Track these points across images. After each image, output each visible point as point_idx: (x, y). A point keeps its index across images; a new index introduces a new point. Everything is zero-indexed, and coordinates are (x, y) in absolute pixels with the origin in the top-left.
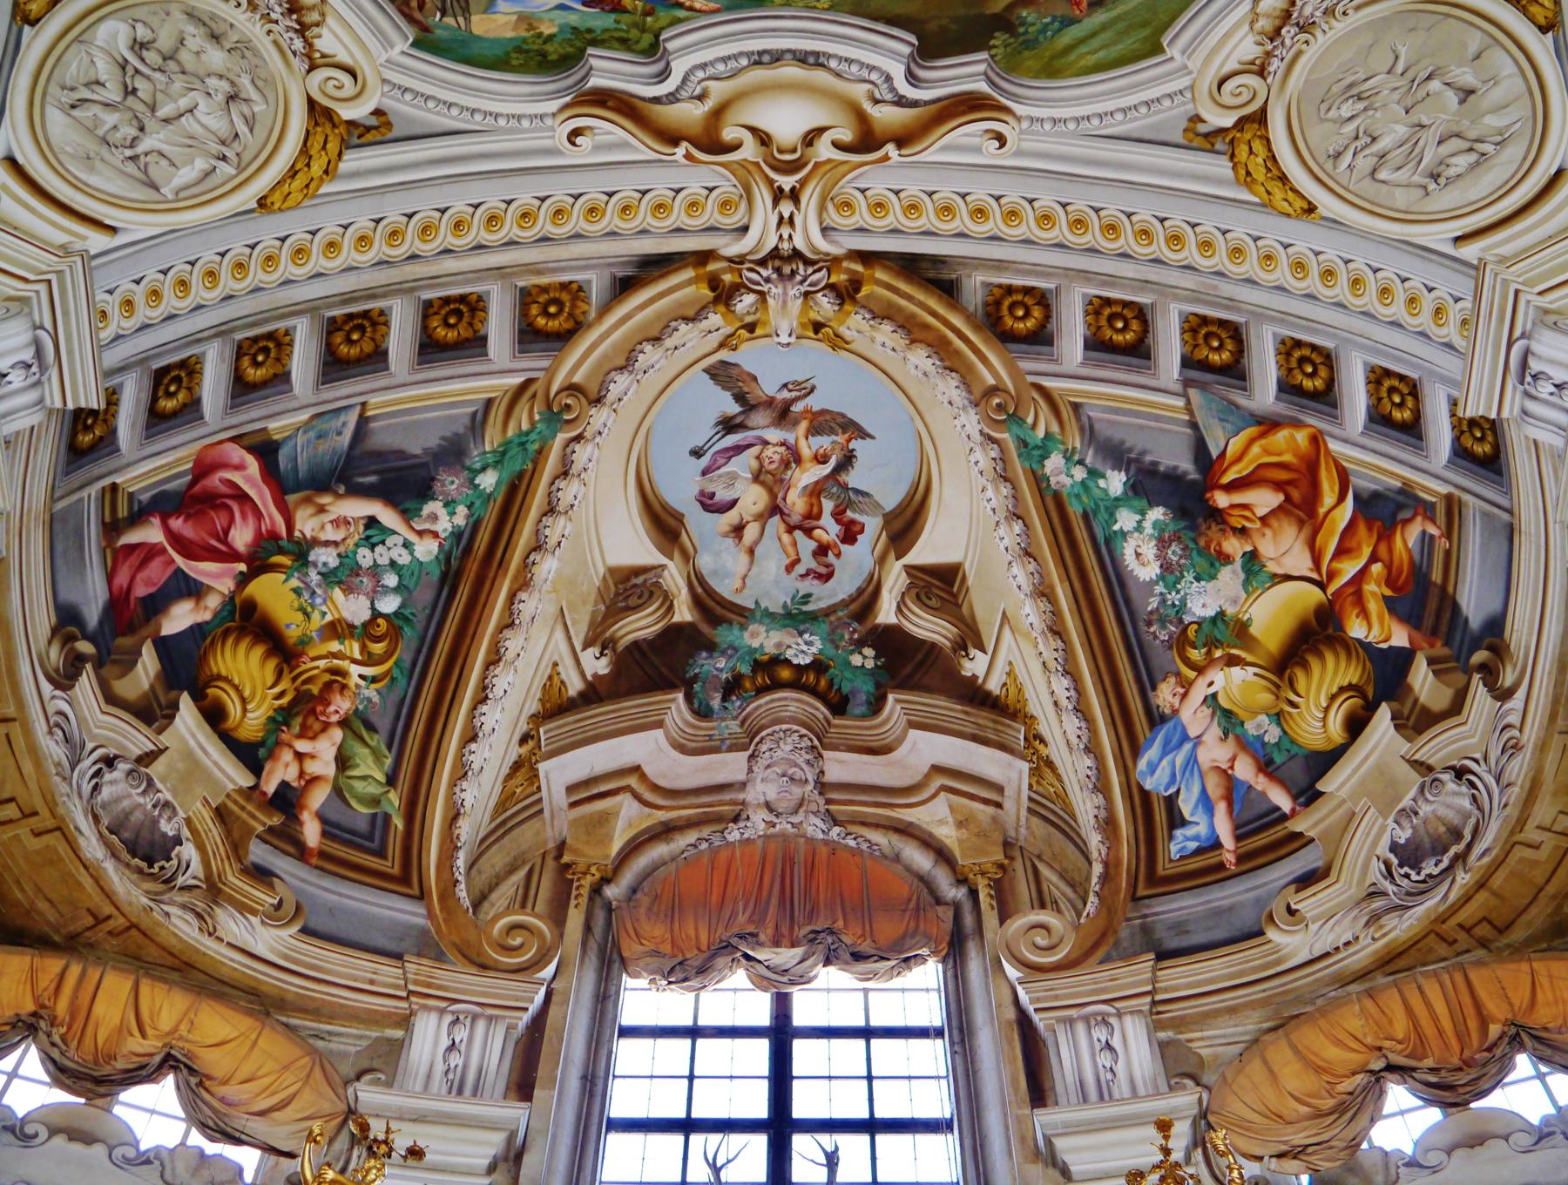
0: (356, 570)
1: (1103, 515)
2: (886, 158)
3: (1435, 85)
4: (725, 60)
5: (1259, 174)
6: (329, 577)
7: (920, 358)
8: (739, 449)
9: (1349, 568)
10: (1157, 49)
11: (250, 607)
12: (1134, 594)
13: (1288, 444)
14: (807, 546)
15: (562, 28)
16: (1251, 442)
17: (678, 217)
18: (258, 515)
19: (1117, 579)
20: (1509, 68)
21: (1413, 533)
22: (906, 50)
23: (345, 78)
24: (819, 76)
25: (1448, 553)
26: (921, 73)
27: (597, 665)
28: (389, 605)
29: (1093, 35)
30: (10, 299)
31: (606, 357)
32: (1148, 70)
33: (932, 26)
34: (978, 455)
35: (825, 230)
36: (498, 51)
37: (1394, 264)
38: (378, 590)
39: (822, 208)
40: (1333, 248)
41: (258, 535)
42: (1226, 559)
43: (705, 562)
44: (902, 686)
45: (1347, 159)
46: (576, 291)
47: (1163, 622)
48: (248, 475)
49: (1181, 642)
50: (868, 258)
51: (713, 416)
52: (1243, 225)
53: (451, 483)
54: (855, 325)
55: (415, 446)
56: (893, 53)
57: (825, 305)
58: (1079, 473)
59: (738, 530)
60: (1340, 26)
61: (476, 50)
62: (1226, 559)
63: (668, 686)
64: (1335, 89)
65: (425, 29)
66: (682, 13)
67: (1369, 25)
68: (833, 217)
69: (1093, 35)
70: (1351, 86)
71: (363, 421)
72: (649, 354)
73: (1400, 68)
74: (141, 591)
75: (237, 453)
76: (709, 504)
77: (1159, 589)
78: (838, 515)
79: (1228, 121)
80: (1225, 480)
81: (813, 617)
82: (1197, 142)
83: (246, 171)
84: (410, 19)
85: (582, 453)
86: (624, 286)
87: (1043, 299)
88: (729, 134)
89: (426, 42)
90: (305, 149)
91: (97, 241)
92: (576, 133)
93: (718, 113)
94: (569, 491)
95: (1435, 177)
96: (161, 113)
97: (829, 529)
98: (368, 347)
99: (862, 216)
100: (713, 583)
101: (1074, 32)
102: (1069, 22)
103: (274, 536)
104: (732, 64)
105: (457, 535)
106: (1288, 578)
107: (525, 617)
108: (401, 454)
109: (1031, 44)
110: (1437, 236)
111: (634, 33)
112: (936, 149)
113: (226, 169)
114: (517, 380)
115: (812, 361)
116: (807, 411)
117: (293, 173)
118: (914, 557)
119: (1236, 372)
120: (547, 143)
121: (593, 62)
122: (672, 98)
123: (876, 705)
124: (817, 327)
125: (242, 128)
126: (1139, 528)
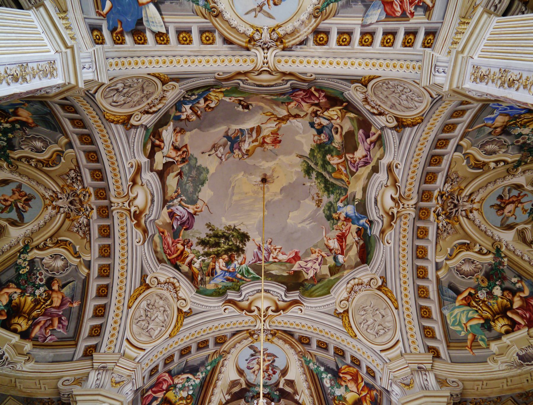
0: (185, 387)
1: (320, 374)
2: (281, 314)
3: (378, 312)
4: (252, 292)
5: (347, 325)
6: (180, 389)
7: (287, 346)
8: (254, 359)
9: (364, 394)
10: (329, 293)
11: (166, 398)
12: (326, 389)
13: (353, 370)
14: (266, 374)
15: (223, 286)
16: (346, 367)
17: (243, 324)
18: (168, 382)
19: (323, 386)
20: (390, 314)
21: (374, 393)
22: (284, 289)
23: (184, 301)
24: (269, 295)
25: (380, 399)
26: (287, 295)
27: (228, 397)
28: (191, 392)
29: (318, 288)
30: (128, 376)
31: (230, 346)
32: (327, 297)
33: (289, 284)
34: (297, 362)
35: (270, 326)
36: (211, 292)
37: (370, 353)
38: (189, 390)
39: (269, 322)
40: (360, 346)
41: (168, 386)
42: (342, 386)
43: (248, 378)
44: (284, 398)
45: (362, 325)
46: (225, 336)
47: (331, 395)
48: (167, 377)
49: (334, 399)
50: (277, 330)
51: (250, 354)
52: (344, 337)
53: (202, 369)
54: (275, 340)
55: (196, 364)
56: (282, 290)
57: (270, 337)
58: (316, 367)
59: (254, 372)
60: (362, 293)
61: (207, 292)
62: (342, 386)
63: (241, 398)
64: (361, 307)
65: (198, 289)
66: (244, 282)
67: (366, 295)
68: (271, 324)
69: (318, 288)
70: (363, 307)
71: (187, 362)
72: (238, 345)
73: (372, 306)
74: (147, 403)
75: (164, 374)
76: (249, 368)
77: (330, 389)
78: (272, 370)
79: (342, 311)
80: (342, 372)
81: (268, 386)
82: (336, 315)
83: (167, 328)
84: (195, 287)
85: (226, 362)
86: (234, 334)
87: (309, 338)
88: (253, 308)
89: (199, 292)
90: (177, 321)
91: (142, 353)
92: (225, 309)
93: (251, 304)
94: (223, 369)
95: (377, 334)
96: (152, 319)
97: (270, 372)
98: (188, 351)
99: (277, 324)
100: (250, 381)
101: (315, 288)
102: (314, 285)
103: (170, 385)
104: (253, 293)
105: (203, 378)
106: (353, 391)
107: (215, 393)
108: (193, 365)
109: (307, 290)
110: (377, 348)
111: (236, 287)
112: (289, 313)
113: (164, 329)
114: (214, 351)
115: (268, 345)
116: (266, 353)
117: (175, 326)
118: (286, 377)
119: (343, 356)
120: (220, 312)
121: (228, 293)
122: (242, 300)
123: (279, 401)
124: (268, 340)
125: (166, 318)
126: (326, 377)
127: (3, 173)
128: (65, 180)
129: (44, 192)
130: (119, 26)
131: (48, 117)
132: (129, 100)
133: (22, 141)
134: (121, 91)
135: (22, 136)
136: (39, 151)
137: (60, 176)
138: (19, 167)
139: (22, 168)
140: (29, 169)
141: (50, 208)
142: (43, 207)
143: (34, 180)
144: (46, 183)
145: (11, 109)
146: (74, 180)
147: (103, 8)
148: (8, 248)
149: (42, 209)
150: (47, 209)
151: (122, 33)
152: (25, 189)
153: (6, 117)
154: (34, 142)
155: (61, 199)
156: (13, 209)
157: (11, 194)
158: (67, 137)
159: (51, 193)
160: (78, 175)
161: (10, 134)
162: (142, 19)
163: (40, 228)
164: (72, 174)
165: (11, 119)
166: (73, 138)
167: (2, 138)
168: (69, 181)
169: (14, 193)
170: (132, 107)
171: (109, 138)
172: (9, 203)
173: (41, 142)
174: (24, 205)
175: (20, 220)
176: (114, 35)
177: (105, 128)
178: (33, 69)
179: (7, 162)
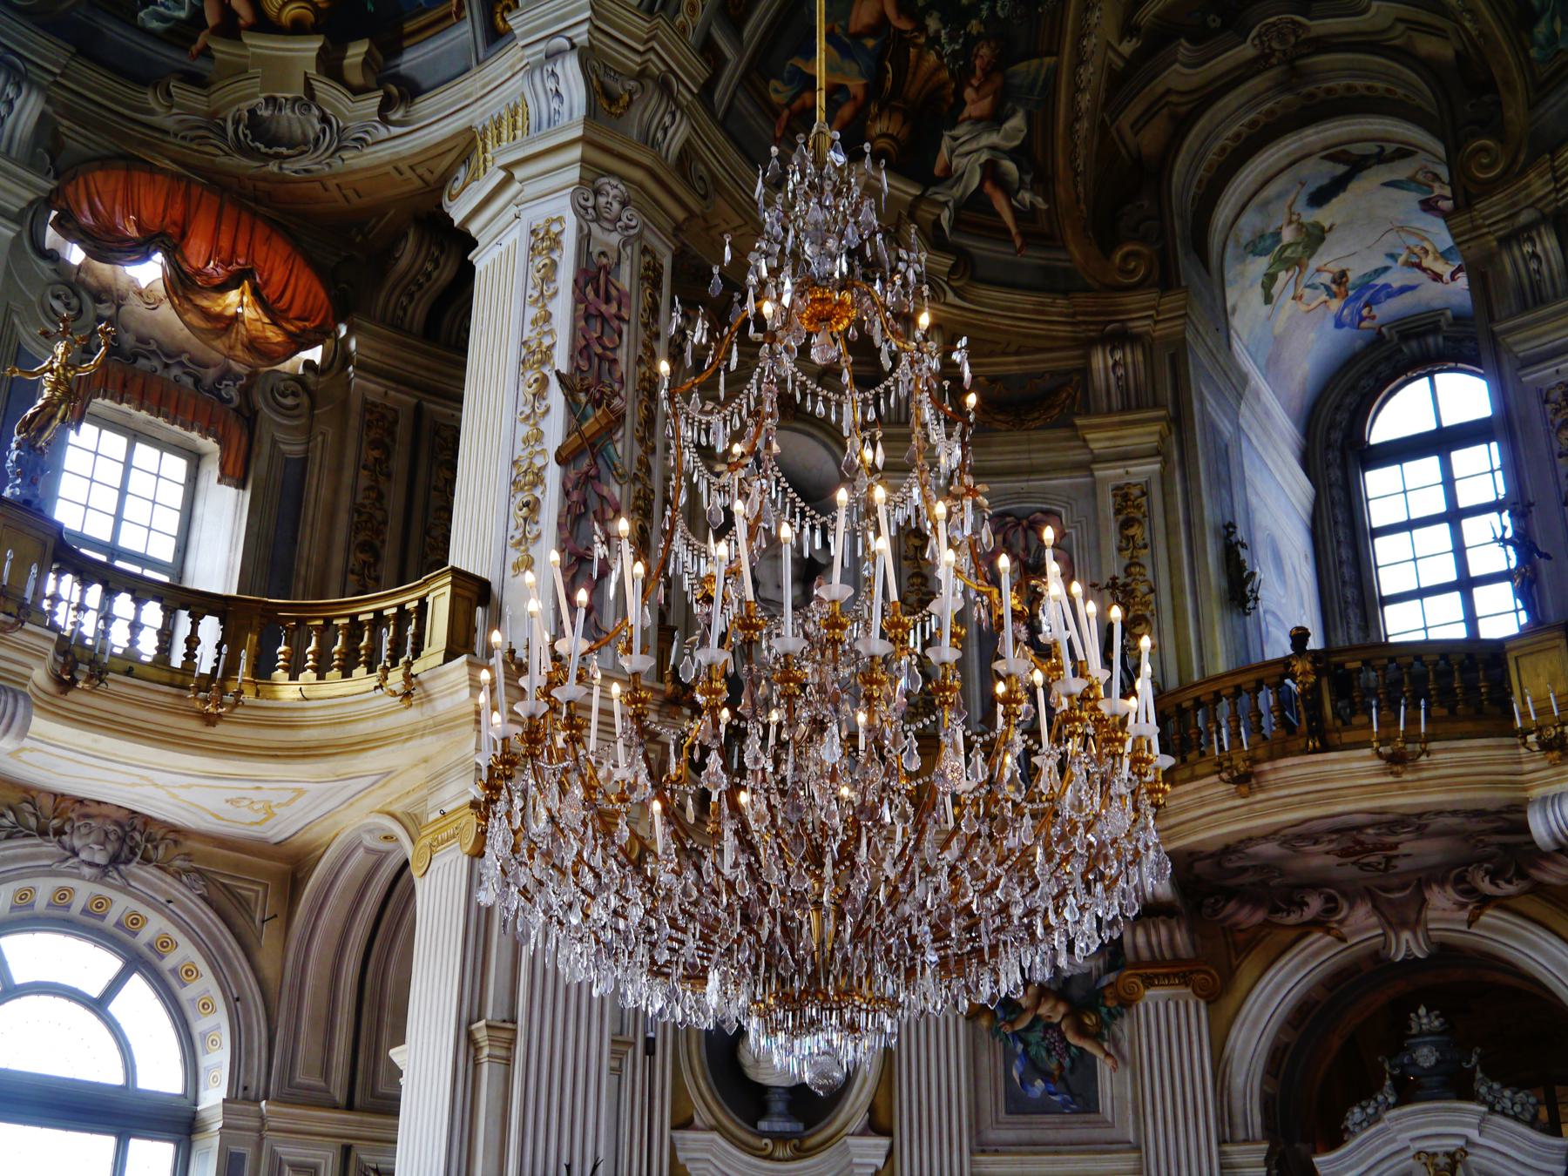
145: (864, 47)
165: (904, 25)
167: (984, 13)
178: (535, 322)
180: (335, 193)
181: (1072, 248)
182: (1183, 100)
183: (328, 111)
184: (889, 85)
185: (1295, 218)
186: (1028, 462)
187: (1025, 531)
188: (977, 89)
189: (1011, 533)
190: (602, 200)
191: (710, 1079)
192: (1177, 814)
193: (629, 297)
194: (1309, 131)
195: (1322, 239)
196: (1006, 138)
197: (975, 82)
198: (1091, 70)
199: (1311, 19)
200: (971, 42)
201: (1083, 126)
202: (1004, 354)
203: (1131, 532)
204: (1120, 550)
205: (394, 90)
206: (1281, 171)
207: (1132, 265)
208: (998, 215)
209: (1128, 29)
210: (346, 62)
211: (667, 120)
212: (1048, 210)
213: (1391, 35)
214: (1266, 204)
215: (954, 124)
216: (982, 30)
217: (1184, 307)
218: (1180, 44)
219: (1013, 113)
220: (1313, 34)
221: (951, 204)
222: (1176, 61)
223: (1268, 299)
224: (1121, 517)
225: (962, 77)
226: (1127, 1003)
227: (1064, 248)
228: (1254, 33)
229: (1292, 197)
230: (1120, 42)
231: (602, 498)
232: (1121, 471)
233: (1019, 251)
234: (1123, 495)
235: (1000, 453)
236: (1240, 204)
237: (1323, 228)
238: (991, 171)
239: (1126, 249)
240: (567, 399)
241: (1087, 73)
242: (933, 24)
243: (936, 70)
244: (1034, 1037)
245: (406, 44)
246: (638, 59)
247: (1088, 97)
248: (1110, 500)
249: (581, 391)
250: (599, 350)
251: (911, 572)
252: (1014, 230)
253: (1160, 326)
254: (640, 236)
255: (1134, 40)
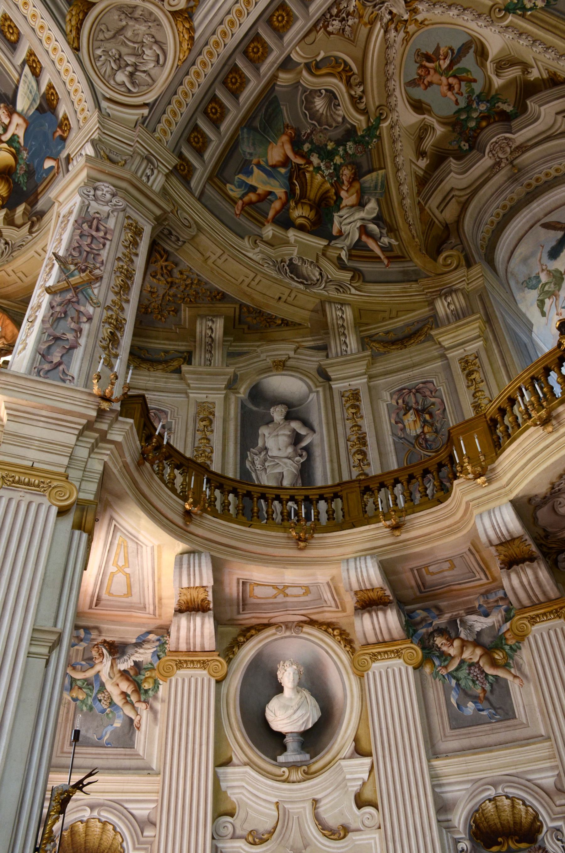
127: (400, 118)
128: (354, 29)
129: (397, 45)
130: (57, 134)
131: (257, 123)
132: (147, 40)
133: (331, 126)
134: (135, 66)
135: (321, 131)
136: (331, 96)
137: (353, 41)
138: (377, 104)
139: (376, 99)
140: (372, 90)
141: (420, 18)
142: (426, 28)
143: (386, 73)
144: (379, 52)
145: (279, 172)
146: (344, 15)
147: (52, 168)
148: (524, 37)
149: (430, 27)
150: (425, 20)
151: (60, 126)
152: (413, 72)
153: (300, 169)
154: (321, 111)
155: (391, 13)
156: (458, 69)
157: (435, 86)
158: (275, 77)
159: (393, 33)
160: (331, 16)
161: (329, 147)
162: (37, 109)
163: (464, 10)
164: (336, 25)
166: (269, 69)
167: (341, 153)
168: (350, 22)
169: (430, 84)
170: (160, 25)
171: (221, 23)
172: (451, 80)
173: (315, 102)
174: (442, 57)
175: (470, 47)
176: (66, 135)
177: (206, 44)
179: (380, 124)
180: (14, 277)
181: (415, 260)
182: (462, 193)
183: (8, 239)
184: (298, 192)
185: (544, 267)
186: (411, 362)
187: (415, 394)
188: (347, 191)
189: (407, 397)
190: (99, 193)
191: (243, 730)
192: (510, 469)
193: (113, 231)
194: (534, 205)
195: (563, 279)
196: (368, 213)
197: (345, 188)
198: (405, 173)
199: (514, 134)
200: (337, 168)
201: (408, 202)
202: (391, 318)
203: (473, 377)
204: (468, 387)
205: (35, 219)
206: (527, 232)
207: (449, 262)
208: (372, 251)
209: (421, 154)
210: (16, 216)
211: (148, 172)
212: (399, 245)
213: (556, 127)
214: (525, 260)
215: (339, 209)
216: (343, 162)
217: (481, 272)
218: (450, 161)
219: (369, 200)
220: (517, 144)
221: (345, 248)
222: (451, 171)
223: (543, 314)
224: (466, 372)
225: (338, 184)
226: (521, 637)
227: (411, 260)
228: (487, 150)
229: (539, 254)
230: (418, 160)
231: (79, 312)
232: (462, 350)
233: (387, 266)
234: (465, 362)
235: (395, 362)
236: (509, 251)
237: (561, 272)
238: (363, 230)
239: (444, 255)
240: (60, 267)
241: (402, 175)
242: (315, 160)
243: (323, 183)
244: (462, 674)
245: (39, 197)
246: (132, 149)
247: (406, 187)
248: (458, 365)
249: (71, 264)
250: (88, 249)
251: (351, 425)
252: (382, 257)
253: (470, 285)
254: (124, 210)
255: (425, 159)
